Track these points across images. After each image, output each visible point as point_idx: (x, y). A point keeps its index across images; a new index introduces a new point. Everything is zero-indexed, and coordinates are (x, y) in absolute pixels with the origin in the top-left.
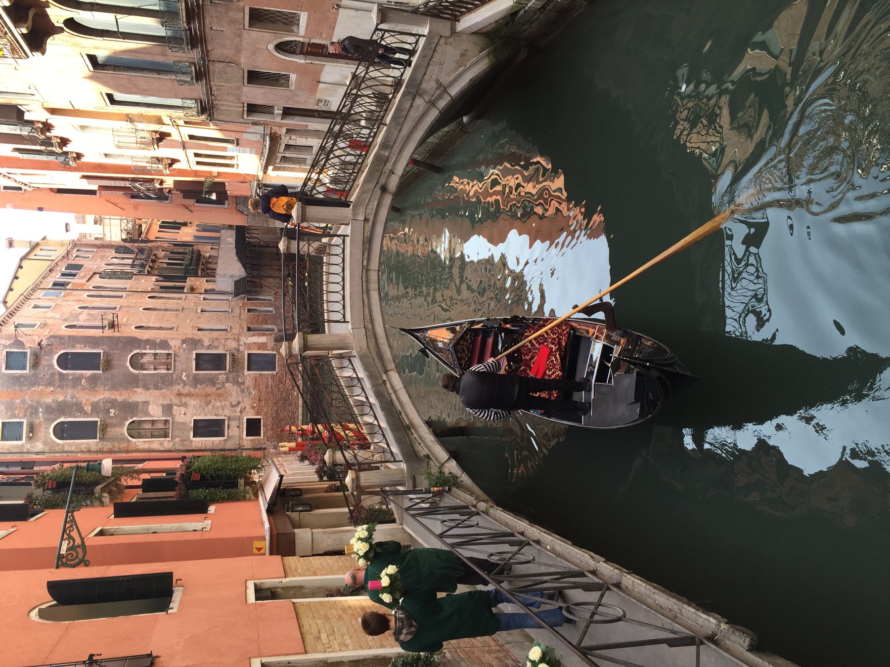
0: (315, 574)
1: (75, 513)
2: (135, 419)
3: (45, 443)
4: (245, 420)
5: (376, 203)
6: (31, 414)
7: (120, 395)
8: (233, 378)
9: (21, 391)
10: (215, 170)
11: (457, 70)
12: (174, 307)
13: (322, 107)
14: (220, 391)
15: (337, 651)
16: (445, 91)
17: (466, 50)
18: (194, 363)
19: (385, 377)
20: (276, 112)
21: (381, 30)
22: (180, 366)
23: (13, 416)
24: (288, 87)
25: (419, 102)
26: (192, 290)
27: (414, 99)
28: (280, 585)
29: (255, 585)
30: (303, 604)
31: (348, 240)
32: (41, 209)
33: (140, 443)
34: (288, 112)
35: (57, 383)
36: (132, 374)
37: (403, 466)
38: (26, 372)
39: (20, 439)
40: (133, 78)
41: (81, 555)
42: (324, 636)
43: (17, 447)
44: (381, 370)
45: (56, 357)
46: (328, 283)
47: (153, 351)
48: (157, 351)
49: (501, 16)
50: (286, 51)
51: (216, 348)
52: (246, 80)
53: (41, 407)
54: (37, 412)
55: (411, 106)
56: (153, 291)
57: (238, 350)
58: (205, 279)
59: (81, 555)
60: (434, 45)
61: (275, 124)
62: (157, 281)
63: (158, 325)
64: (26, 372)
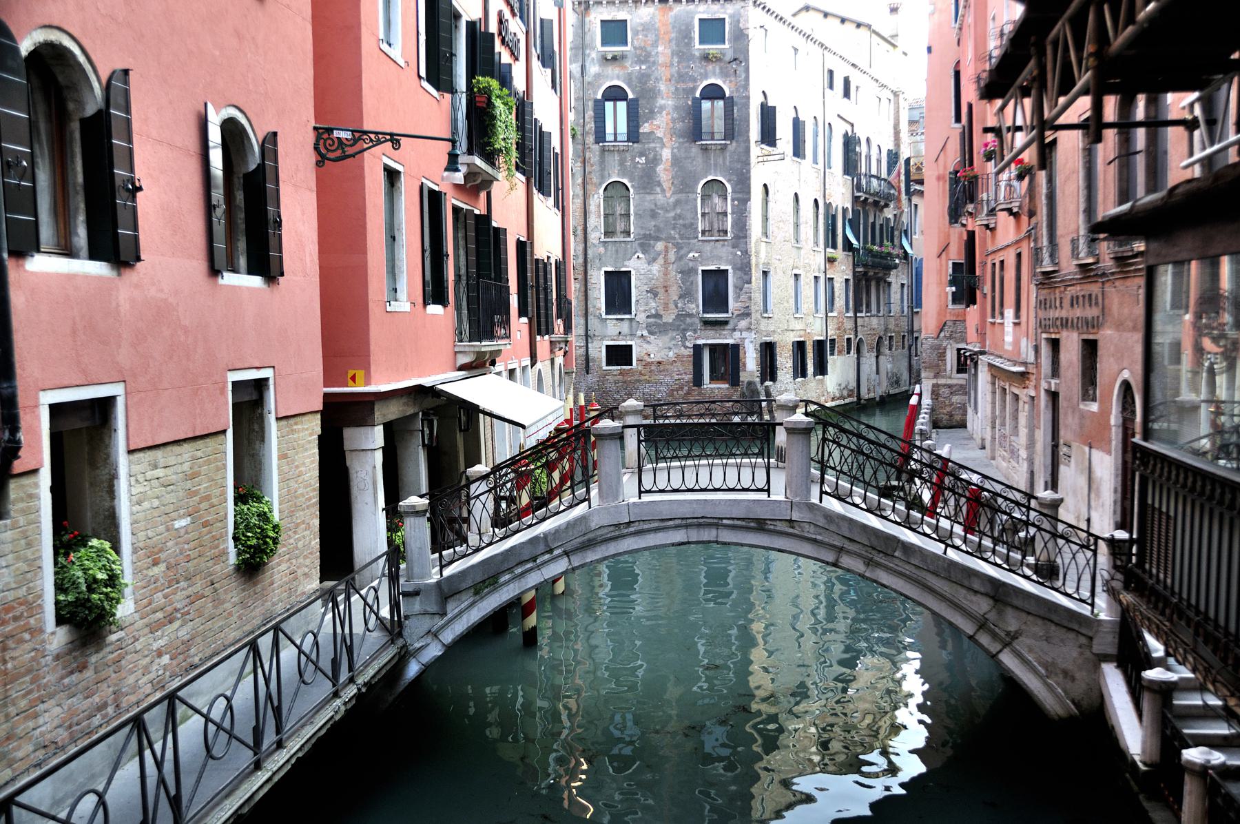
0: (282, 457)
1: (389, 144)
2: (631, 190)
3: (598, 76)
4: (629, 343)
5: (819, 537)
6: (639, 56)
7: (665, 170)
8: (692, 325)
9: (670, 41)
10: (987, 289)
11: (1040, 663)
12: (802, 236)
13: (1063, 450)
14: (672, 306)
15: (130, 491)
16: (1006, 645)
17: (1073, 679)
18: (713, 268)
19: (556, 552)
20: (1053, 382)
21: (1096, 544)
22: (708, 247)
23: (636, 33)
24: (1084, 400)
25: (982, 605)
26: (831, 260)
27: (986, 595)
28: (266, 411)
29: (267, 379)
30: (224, 443)
31: (763, 496)
32: (929, 50)
33: (597, 200)
34: (1054, 396)
35: (682, 86)
36: (697, 183)
37: (434, 577)
38: (697, 46)
39: (603, 44)
40: (1075, 176)
41: (331, 155)
42: (159, 472)
43: (593, 40)
44: (569, 547)
45: (719, 82)
46: (739, 466)
47: (729, 211)
48: (729, 216)
49: (1119, 737)
50: (1125, 397)
51: (737, 297)
52: (1085, 337)
53: (649, 67)
54: (640, 62)
55: (976, 592)
56: (828, 206)
57: (734, 330)
58: (850, 277)
59: (331, 155)
60: (1076, 627)
61: (1038, 380)
62: (845, 211)
63: (770, 215)
64: (697, 46)
